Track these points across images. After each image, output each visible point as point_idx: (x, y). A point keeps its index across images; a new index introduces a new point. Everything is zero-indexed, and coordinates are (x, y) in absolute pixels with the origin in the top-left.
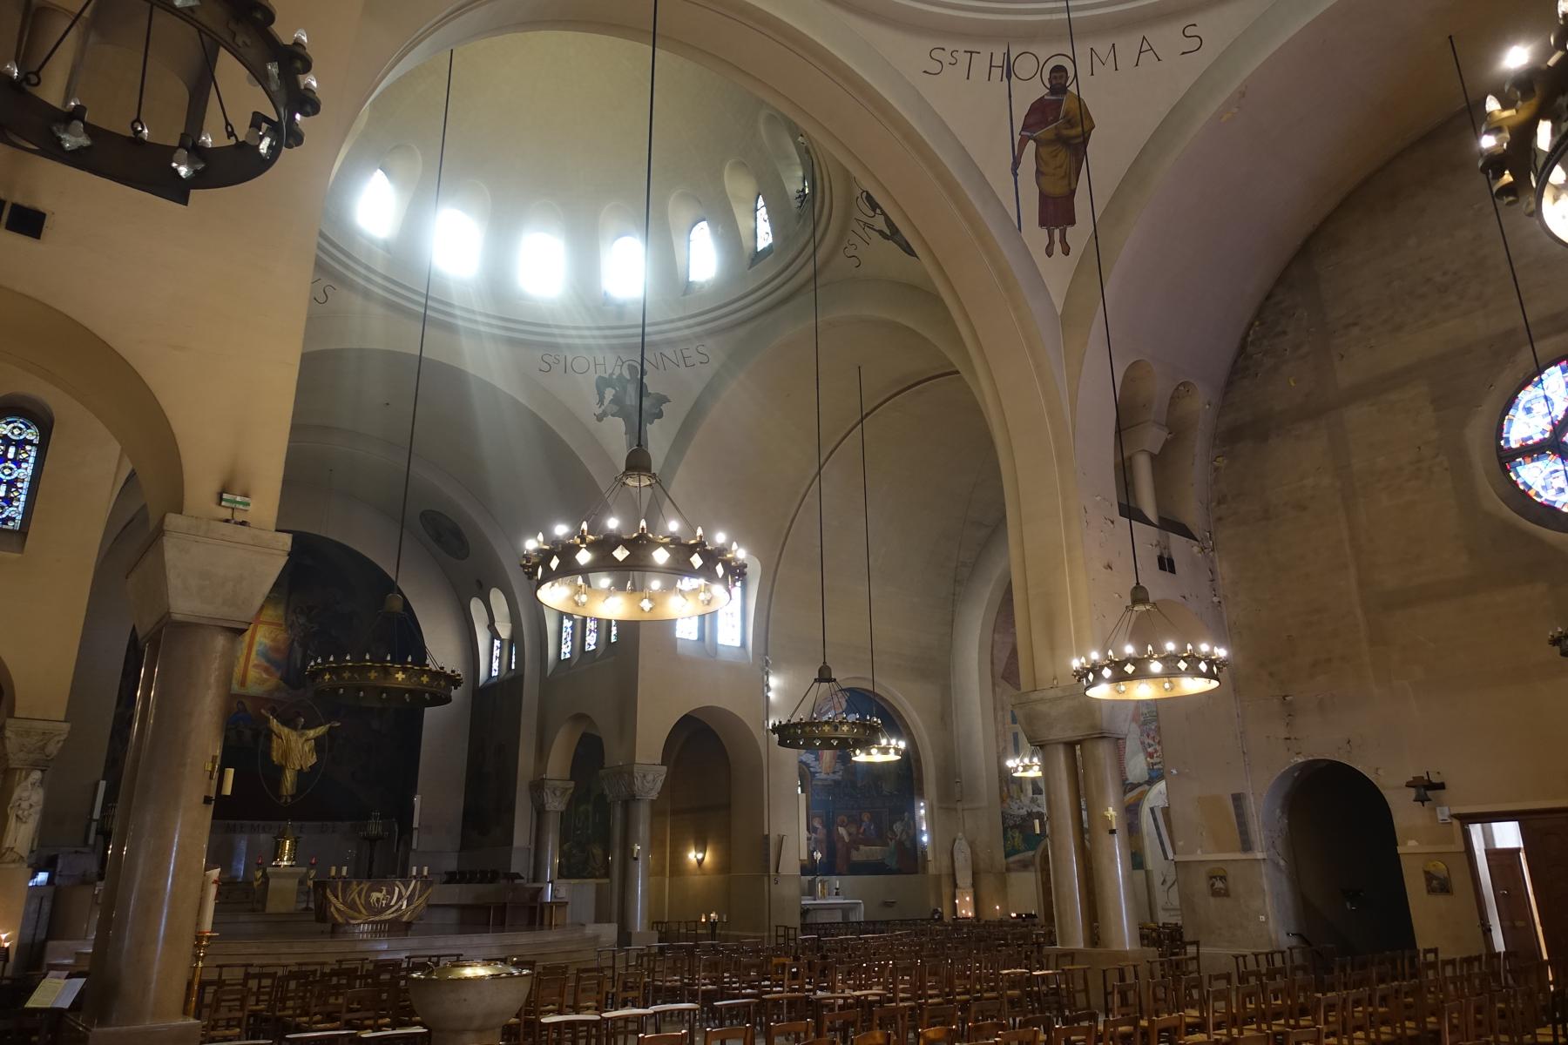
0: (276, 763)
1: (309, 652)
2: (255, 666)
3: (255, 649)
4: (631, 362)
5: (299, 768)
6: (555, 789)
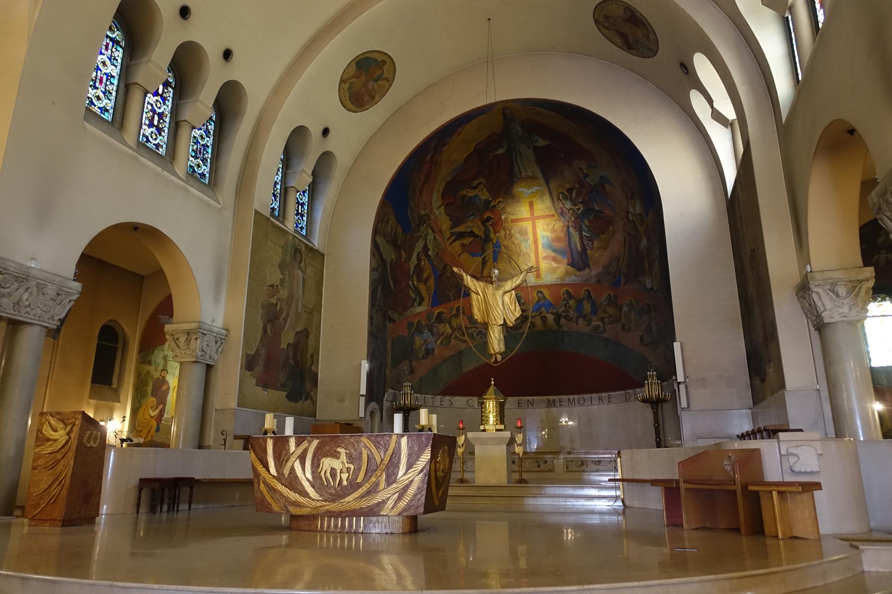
0: (479, 321)
1: (584, 233)
2: (545, 258)
3: (540, 242)
5: (501, 322)
6: (834, 284)
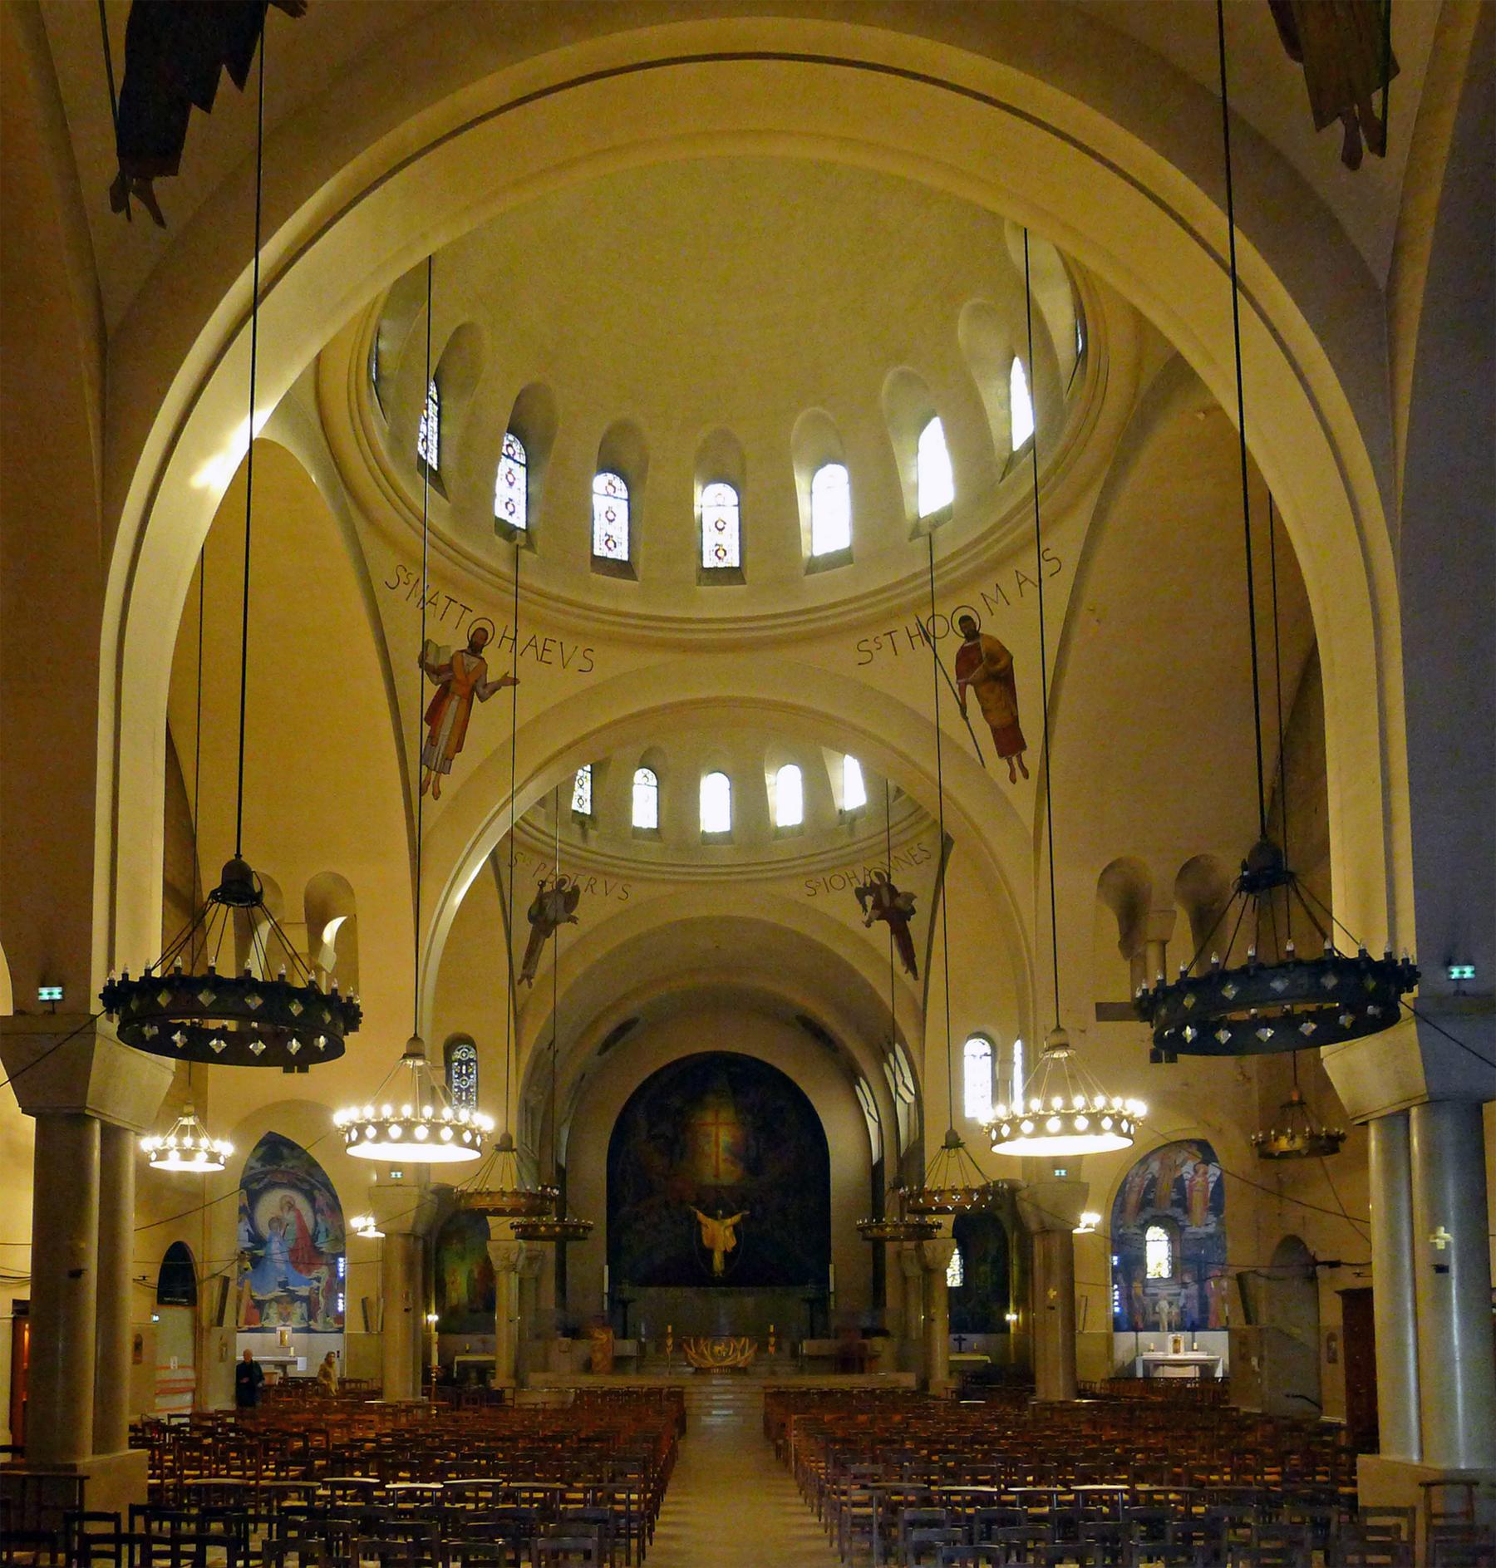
2: (725, 1160)
3: (722, 1144)
4: (877, 870)
